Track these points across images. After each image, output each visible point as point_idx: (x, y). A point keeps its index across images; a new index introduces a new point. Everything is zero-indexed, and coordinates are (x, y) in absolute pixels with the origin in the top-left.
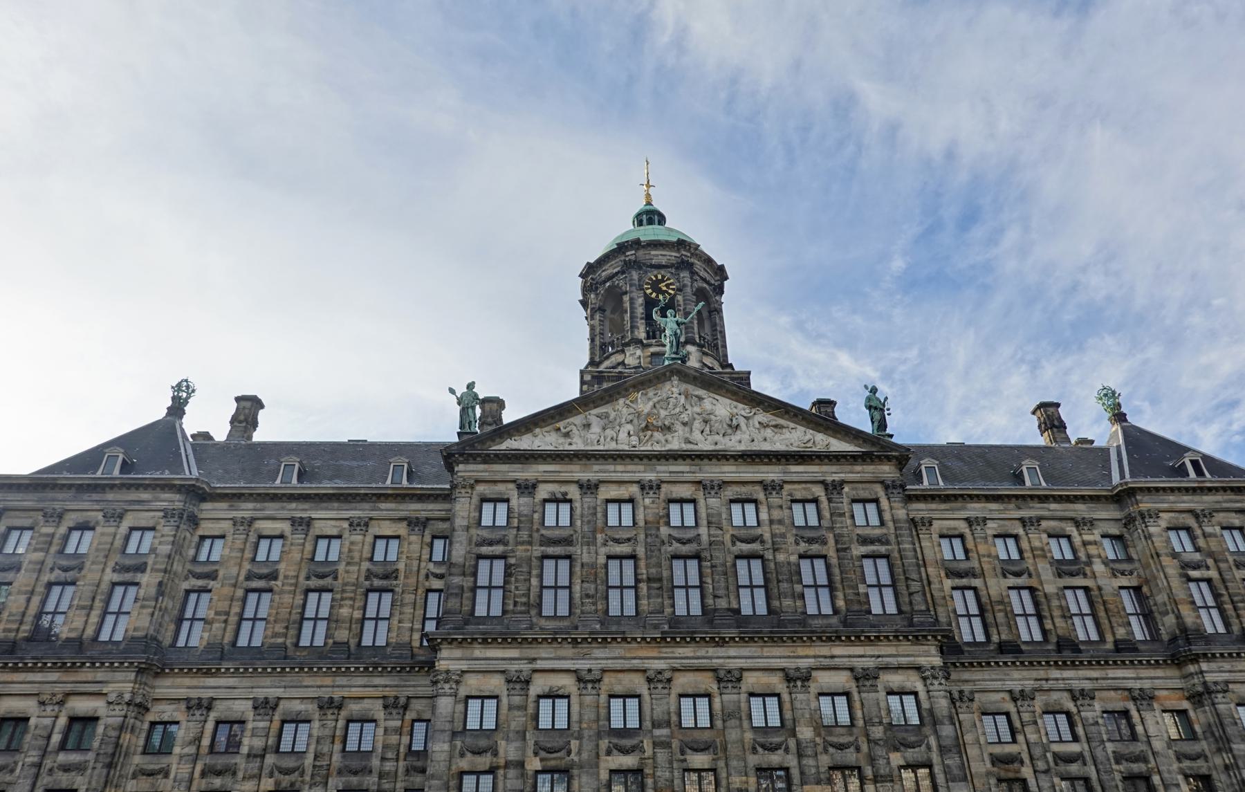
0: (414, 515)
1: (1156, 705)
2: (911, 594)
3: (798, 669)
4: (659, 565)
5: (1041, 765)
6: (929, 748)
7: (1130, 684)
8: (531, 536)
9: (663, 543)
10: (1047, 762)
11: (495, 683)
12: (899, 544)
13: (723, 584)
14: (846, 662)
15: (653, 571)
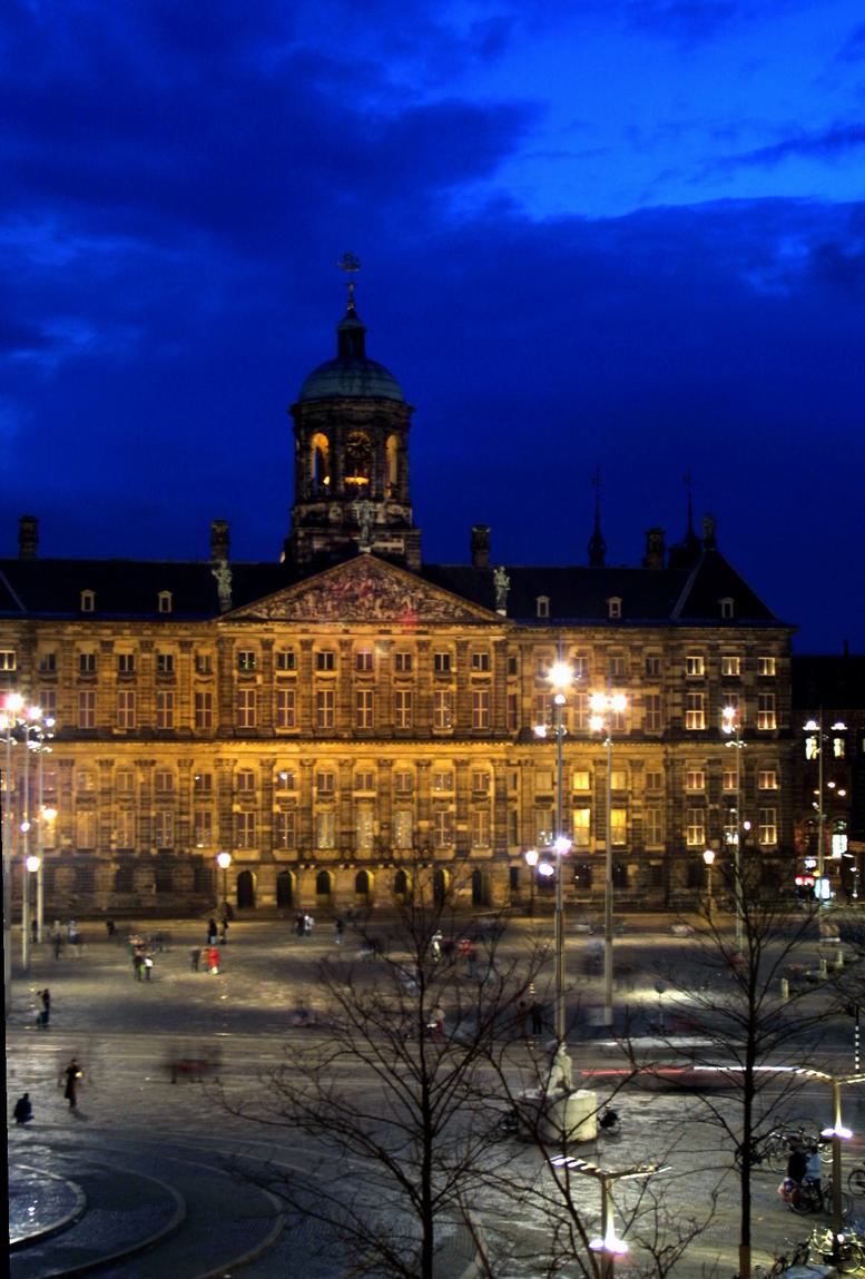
0: (183, 639)
1: (644, 769)
2: (497, 717)
3: (424, 760)
4: (350, 697)
5: (564, 803)
6: (490, 802)
7: (632, 757)
8: (271, 677)
9: (351, 682)
10: (568, 802)
11: (255, 766)
12: (496, 684)
13: (386, 710)
14: (452, 756)
15: (345, 700)
